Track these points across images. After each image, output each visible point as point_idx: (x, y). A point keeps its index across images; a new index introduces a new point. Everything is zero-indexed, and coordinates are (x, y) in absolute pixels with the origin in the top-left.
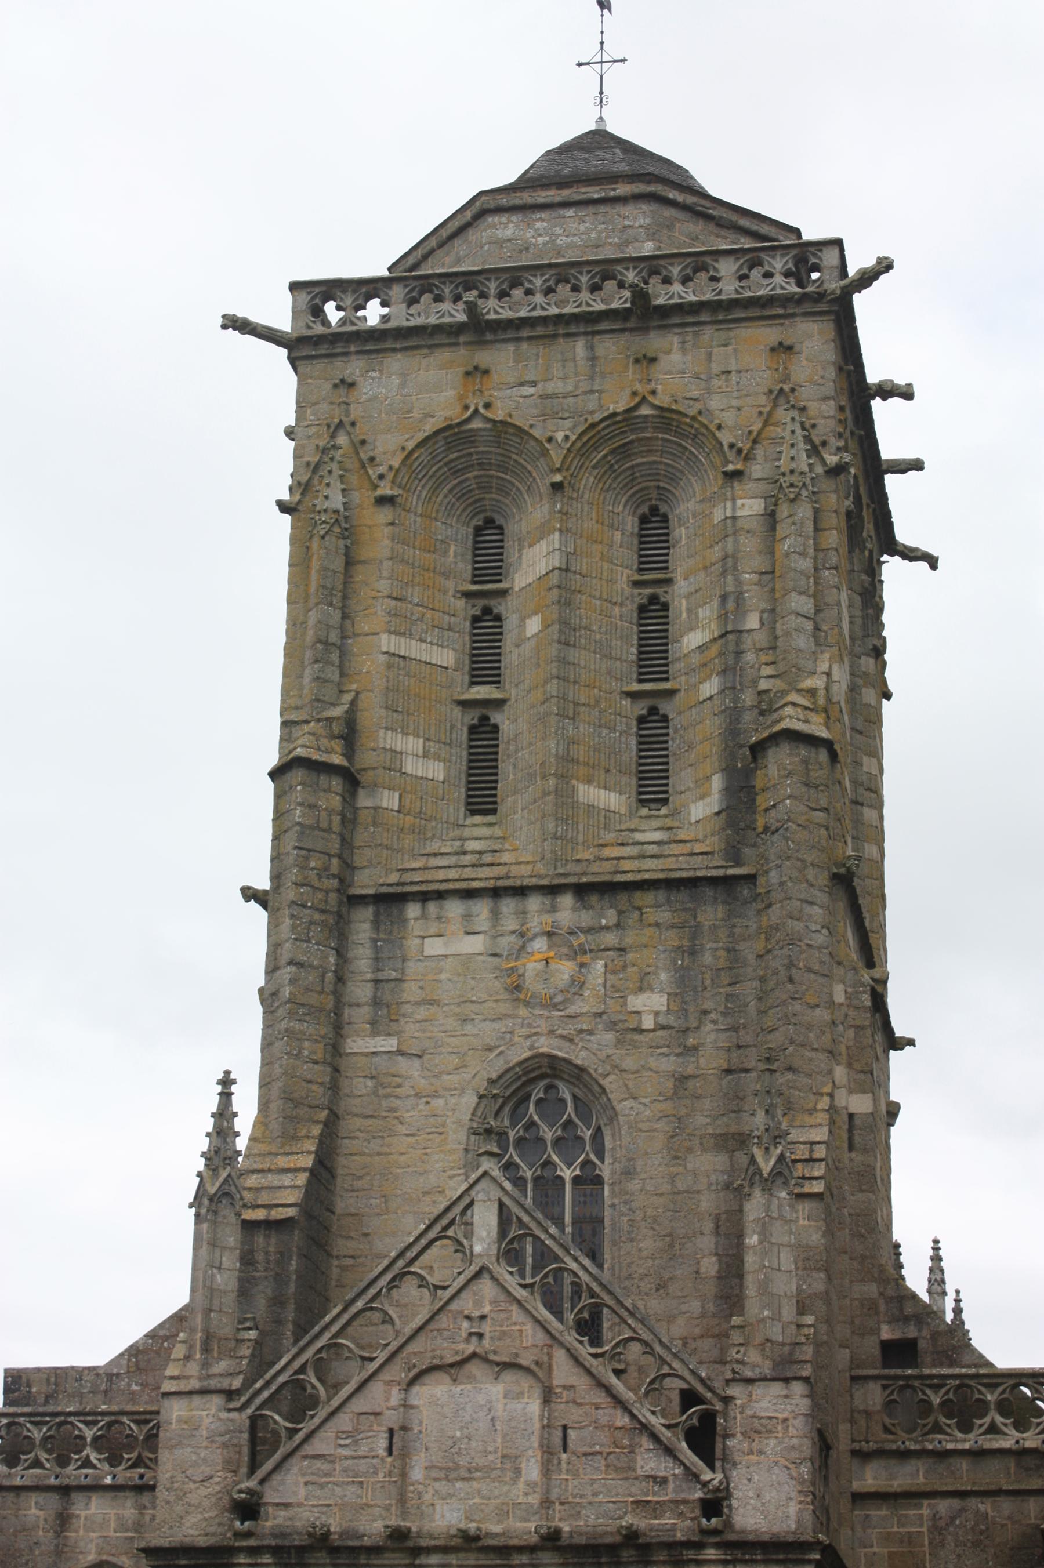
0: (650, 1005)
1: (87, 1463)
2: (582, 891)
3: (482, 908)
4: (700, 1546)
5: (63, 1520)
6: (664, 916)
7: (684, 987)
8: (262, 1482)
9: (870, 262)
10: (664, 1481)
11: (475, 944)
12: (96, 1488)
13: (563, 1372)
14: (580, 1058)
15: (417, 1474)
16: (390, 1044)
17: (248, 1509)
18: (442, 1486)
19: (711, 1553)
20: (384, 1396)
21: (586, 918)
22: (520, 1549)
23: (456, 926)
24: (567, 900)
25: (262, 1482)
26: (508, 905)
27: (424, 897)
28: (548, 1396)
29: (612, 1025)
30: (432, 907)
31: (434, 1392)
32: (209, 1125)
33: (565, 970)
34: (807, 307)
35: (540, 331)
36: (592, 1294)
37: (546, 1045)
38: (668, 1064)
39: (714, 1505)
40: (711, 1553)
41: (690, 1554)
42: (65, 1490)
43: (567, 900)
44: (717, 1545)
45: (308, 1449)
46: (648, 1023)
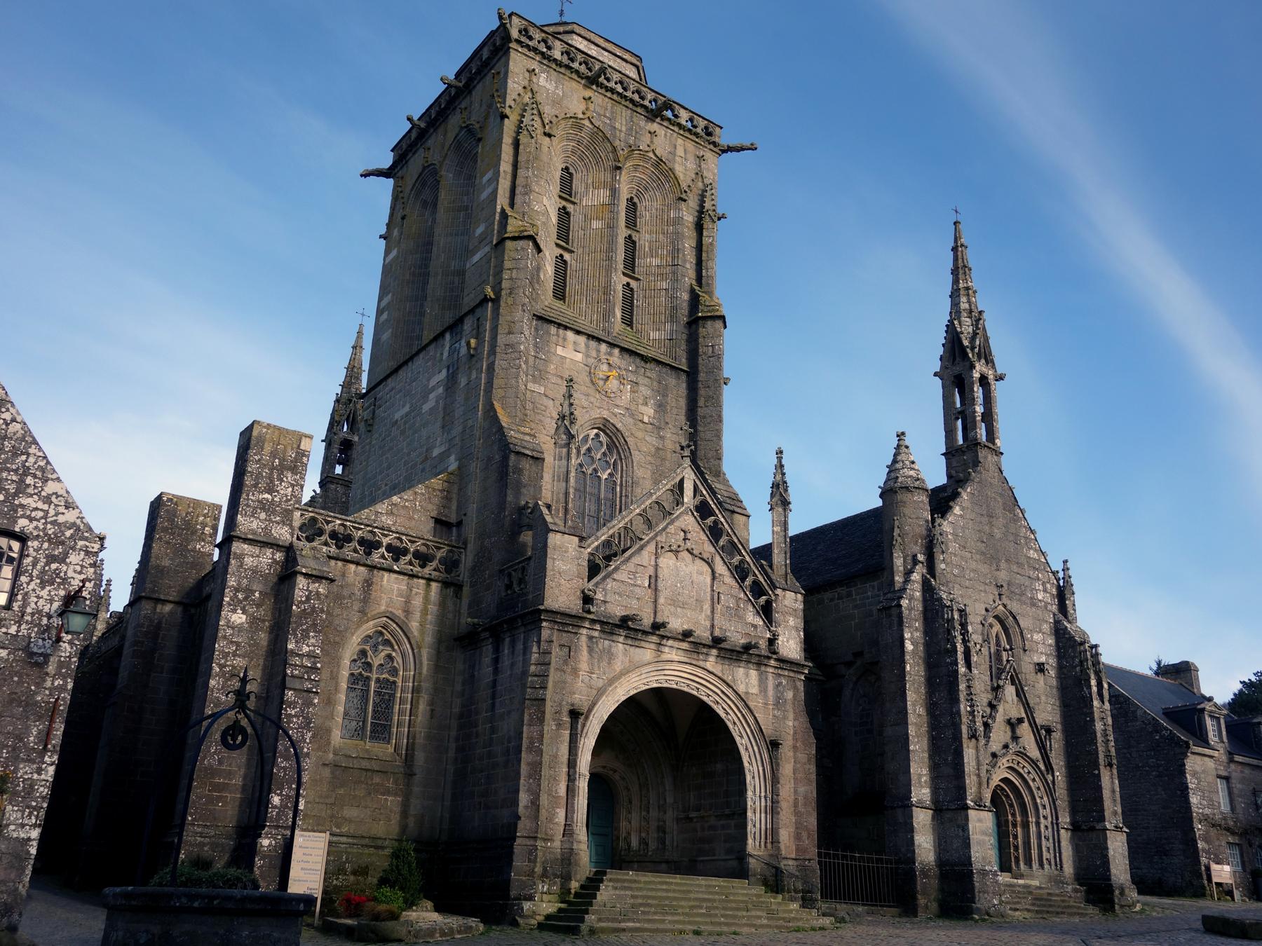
0: (648, 412)
1: (383, 557)
2: (623, 350)
3: (582, 340)
4: (769, 658)
5: (368, 584)
6: (654, 375)
7: (661, 407)
8: (597, 585)
9: (747, 143)
10: (755, 626)
11: (579, 357)
12: (391, 571)
14: (619, 425)
15: (661, 600)
16: (542, 390)
18: (672, 609)
19: (772, 662)
20: (646, 557)
21: (623, 364)
22: (704, 645)
23: (571, 346)
24: (616, 351)
25: (597, 585)
26: (593, 344)
27: (559, 325)
29: (632, 415)
30: (561, 331)
31: (667, 561)
33: (613, 384)
34: (711, 147)
35: (615, 97)
36: (728, 535)
37: (606, 414)
38: (652, 440)
39: (772, 642)
40: (772, 662)
41: (766, 661)
42: (372, 567)
43: (616, 351)
44: (777, 660)
45: (615, 576)
46: (646, 420)
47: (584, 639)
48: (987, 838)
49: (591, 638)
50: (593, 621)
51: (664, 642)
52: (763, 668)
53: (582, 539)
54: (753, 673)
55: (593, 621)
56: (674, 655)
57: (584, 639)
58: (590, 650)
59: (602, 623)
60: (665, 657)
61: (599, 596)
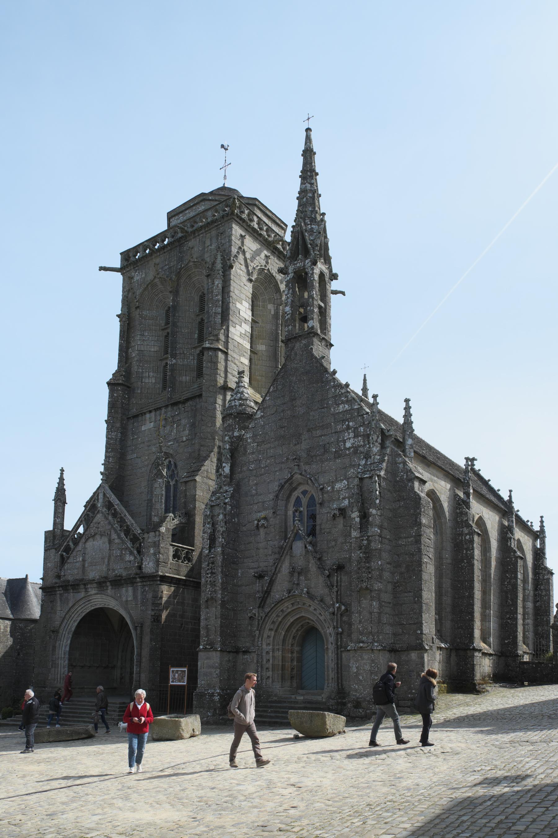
4: (136, 578)
10: (130, 562)
13: (114, 536)
15: (86, 565)
17: (59, 577)
28: (110, 542)
32: (58, 481)
41: (134, 580)
47: (58, 596)
48: (213, 670)
49: (61, 594)
50: (59, 587)
51: (87, 587)
52: (135, 585)
53: (56, 549)
54: (130, 589)
55: (59, 587)
56: (93, 592)
57: (58, 596)
58: (61, 600)
59: (62, 586)
60: (89, 594)
61: (62, 574)
